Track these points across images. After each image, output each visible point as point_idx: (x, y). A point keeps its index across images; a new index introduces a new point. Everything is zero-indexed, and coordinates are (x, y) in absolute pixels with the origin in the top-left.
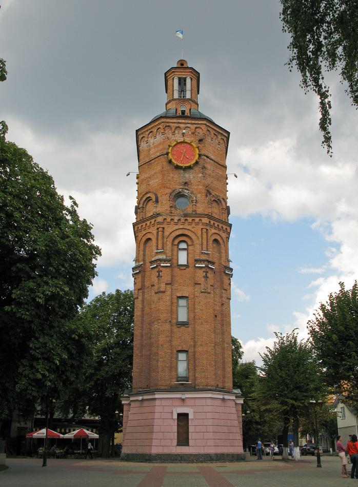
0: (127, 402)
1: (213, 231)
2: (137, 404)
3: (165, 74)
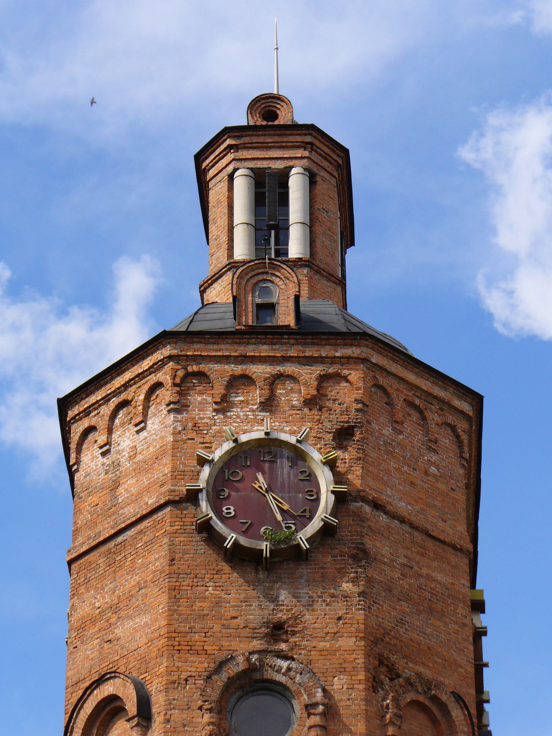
3: (199, 157)
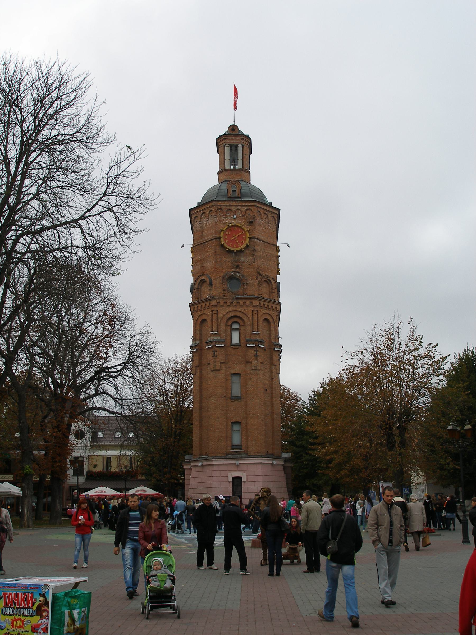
0: (189, 467)
1: (264, 311)
2: (198, 469)
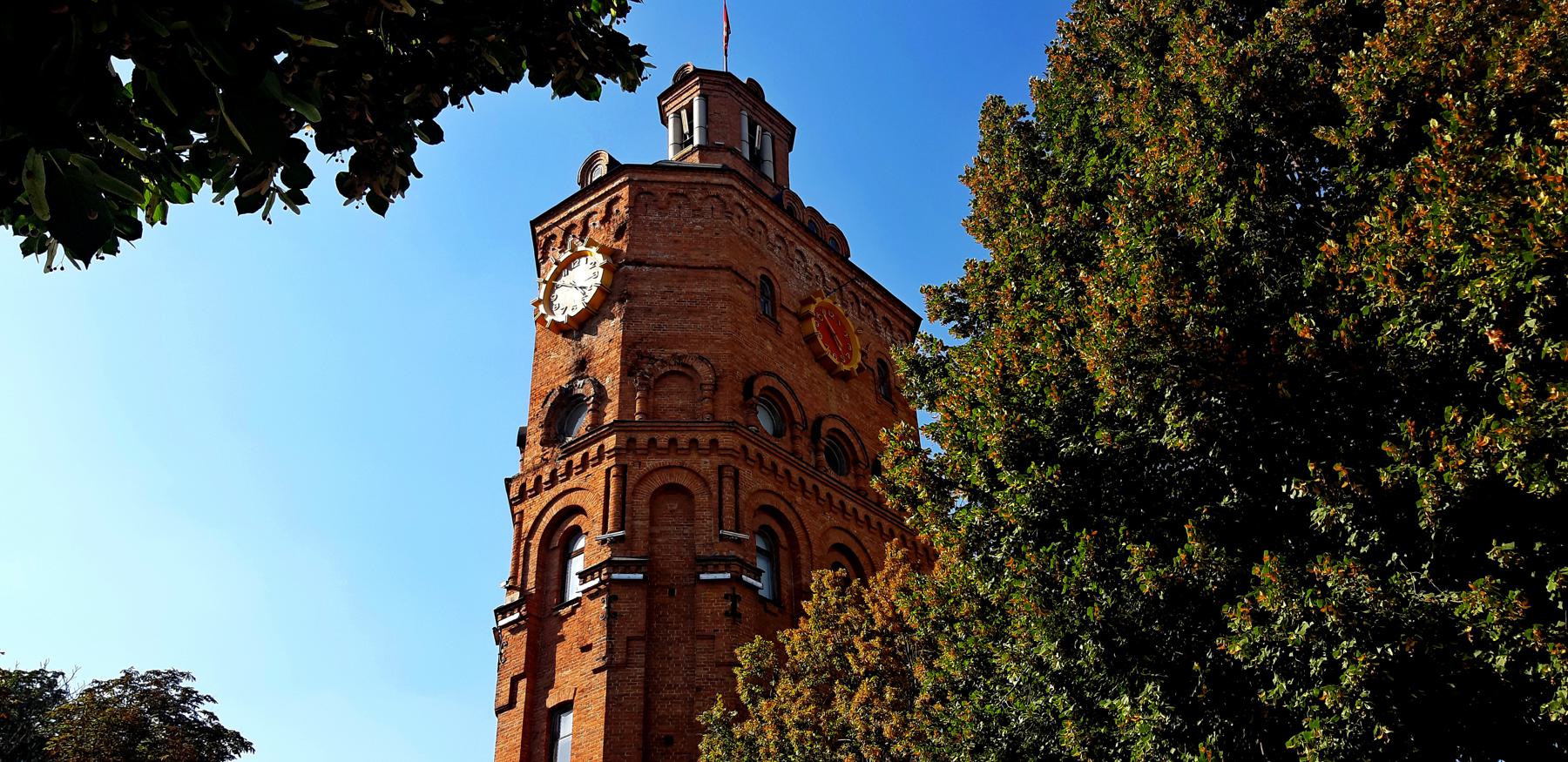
1: (651, 463)
